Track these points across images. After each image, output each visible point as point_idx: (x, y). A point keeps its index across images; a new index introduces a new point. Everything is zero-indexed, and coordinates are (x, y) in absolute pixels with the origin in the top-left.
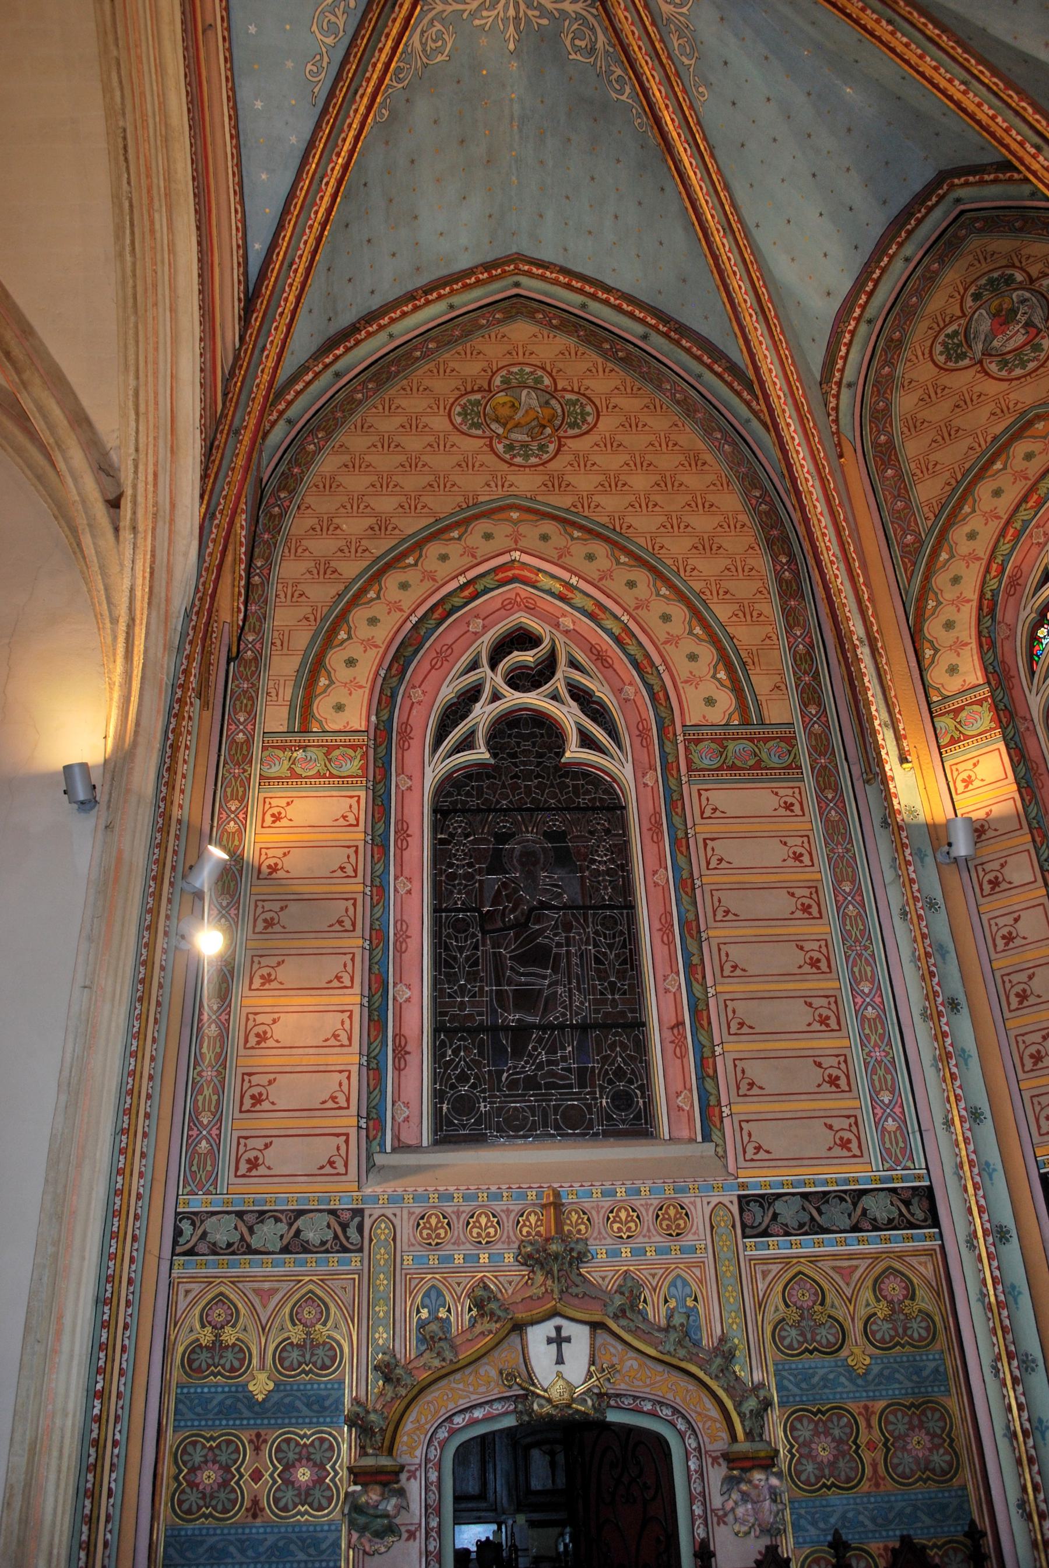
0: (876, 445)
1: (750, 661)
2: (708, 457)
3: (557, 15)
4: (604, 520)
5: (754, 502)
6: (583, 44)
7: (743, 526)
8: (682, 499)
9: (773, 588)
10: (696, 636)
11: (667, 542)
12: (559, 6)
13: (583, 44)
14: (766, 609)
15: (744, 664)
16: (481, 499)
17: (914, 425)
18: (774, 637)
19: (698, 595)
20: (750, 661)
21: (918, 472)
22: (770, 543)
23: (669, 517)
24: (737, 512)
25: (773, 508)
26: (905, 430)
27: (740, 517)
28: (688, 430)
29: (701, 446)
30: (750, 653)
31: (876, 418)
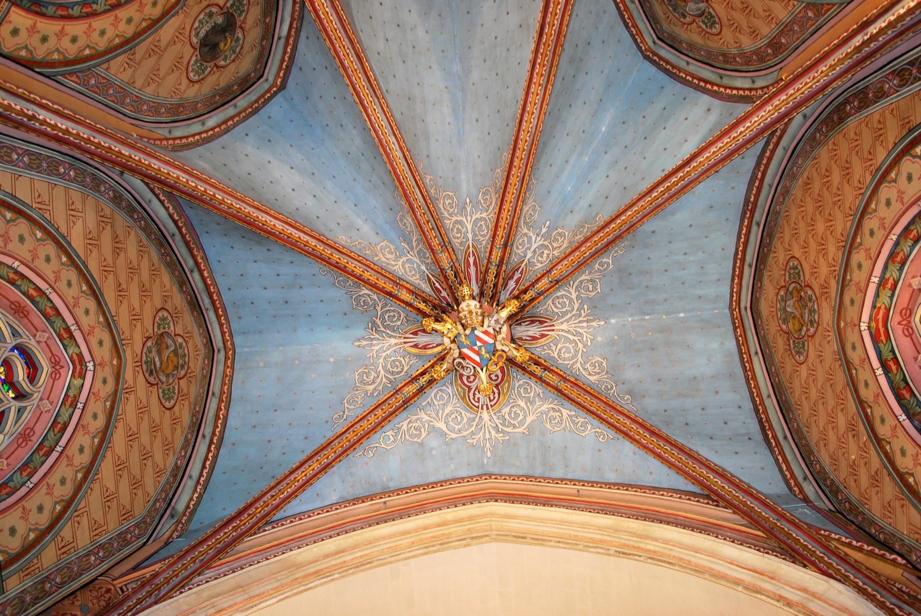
0: (775, 55)
1: (908, 126)
2: (805, 175)
3: (580, 301)
4: (840, 255)
5: (822, 137)
6: (591, 287)
7: (834, 143)
8: (826, 194)
9: (865, 113)
10: (897, 175)
11: (847, 205)
12: (575, 301)
13: (591, 287)
14: (876, 117)
15: (910, 131)
16: (836, 349)
17: (754, 33)
18: (892, 107)
19: (873, 177)
20: (908, 126)
21: (774, 21)
22: (841, 120)
23: (835, 203)
24: (828, 149)
25: (824, 122)
26: (759, 37)
27: (831, 148)
28: (794, 192)
29: (800, 181)
30: (903, 126)
31: (762, 58)
